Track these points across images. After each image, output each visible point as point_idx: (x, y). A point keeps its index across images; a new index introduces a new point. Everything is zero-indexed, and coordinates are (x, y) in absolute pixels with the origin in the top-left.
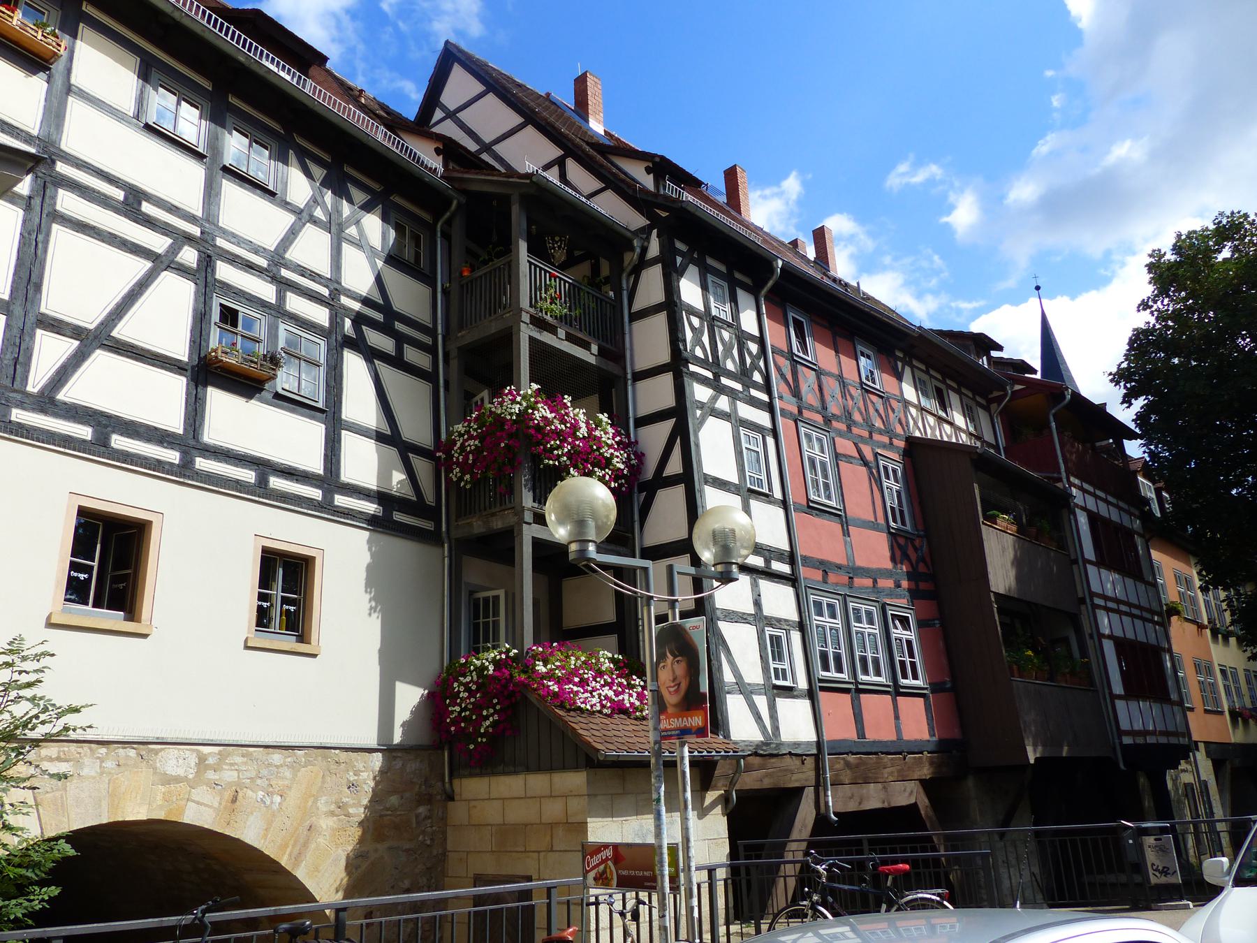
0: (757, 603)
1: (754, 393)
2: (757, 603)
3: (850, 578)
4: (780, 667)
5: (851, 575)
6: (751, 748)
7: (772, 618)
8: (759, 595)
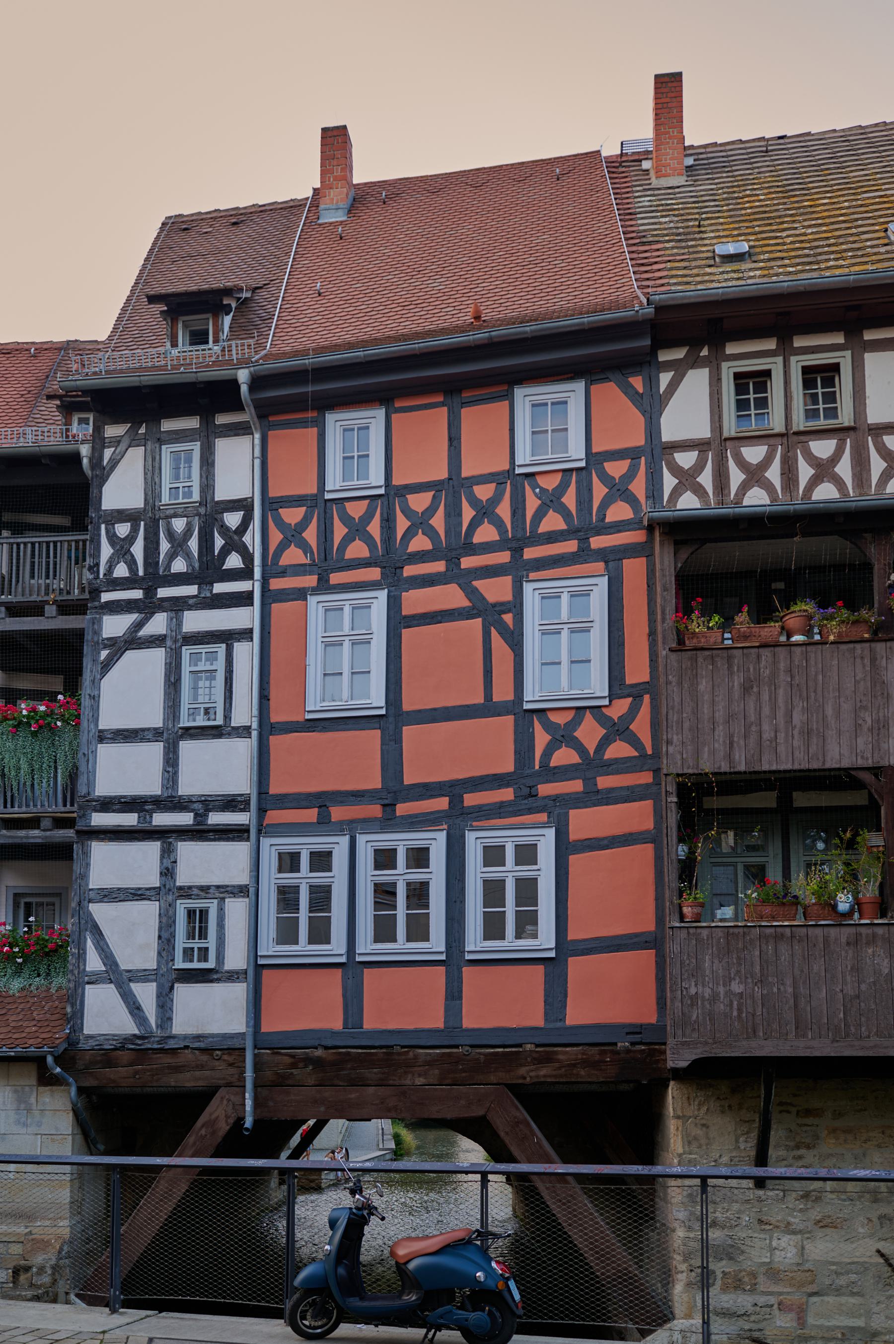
0: (168, 873)
1: (219, 588)
2: (168, 873)
3: (384, 806)
4: (196, 946)
5: (386, 802)
6: (114, 1042)
7: (190, 888)
8: (175, 862)
